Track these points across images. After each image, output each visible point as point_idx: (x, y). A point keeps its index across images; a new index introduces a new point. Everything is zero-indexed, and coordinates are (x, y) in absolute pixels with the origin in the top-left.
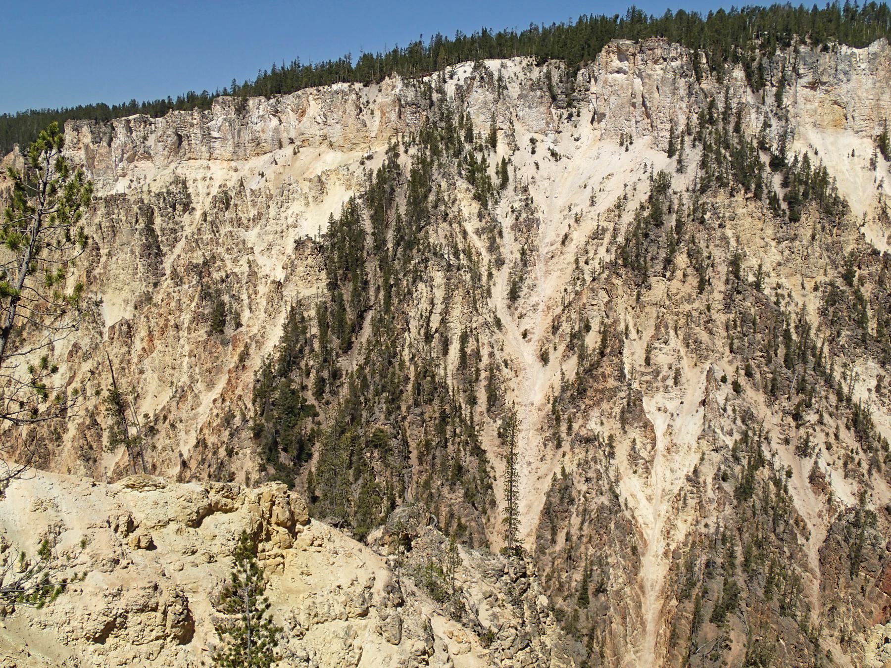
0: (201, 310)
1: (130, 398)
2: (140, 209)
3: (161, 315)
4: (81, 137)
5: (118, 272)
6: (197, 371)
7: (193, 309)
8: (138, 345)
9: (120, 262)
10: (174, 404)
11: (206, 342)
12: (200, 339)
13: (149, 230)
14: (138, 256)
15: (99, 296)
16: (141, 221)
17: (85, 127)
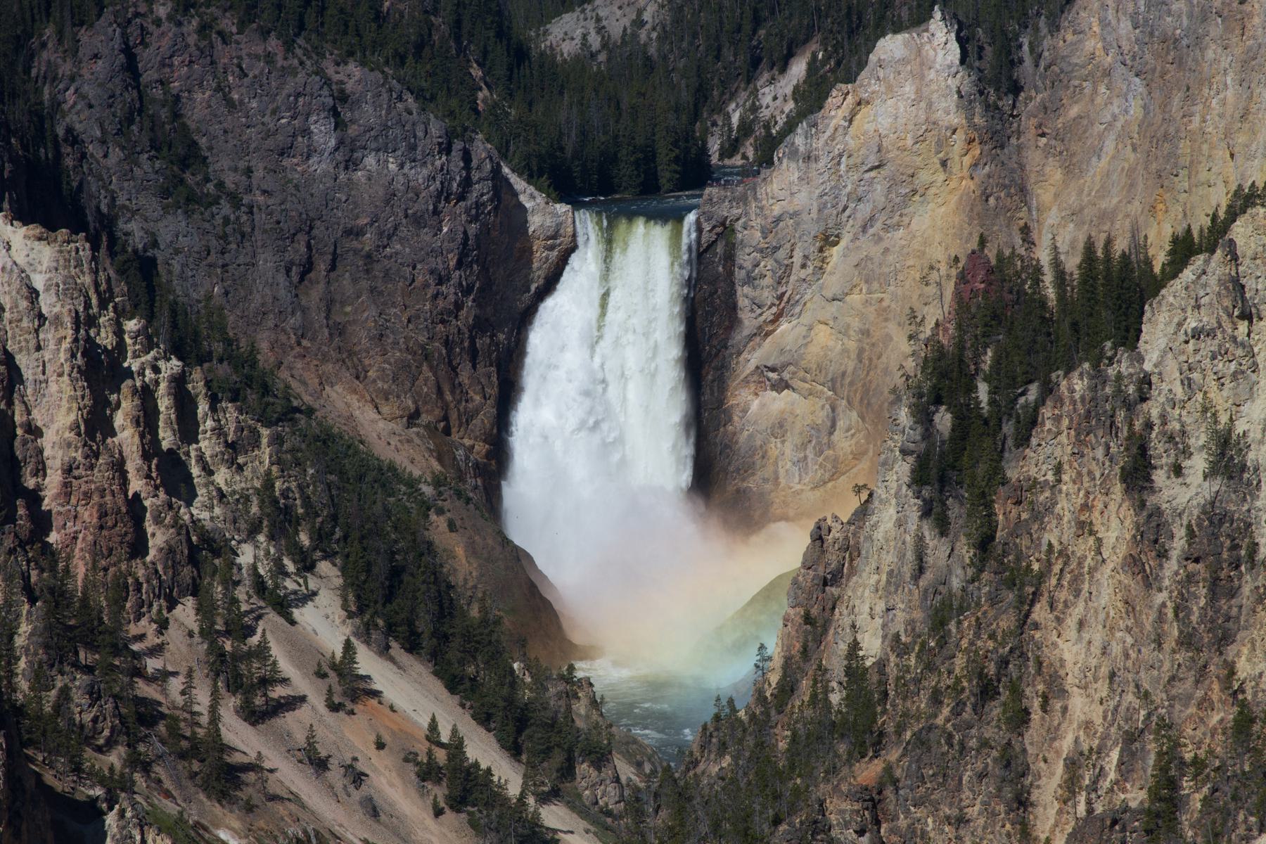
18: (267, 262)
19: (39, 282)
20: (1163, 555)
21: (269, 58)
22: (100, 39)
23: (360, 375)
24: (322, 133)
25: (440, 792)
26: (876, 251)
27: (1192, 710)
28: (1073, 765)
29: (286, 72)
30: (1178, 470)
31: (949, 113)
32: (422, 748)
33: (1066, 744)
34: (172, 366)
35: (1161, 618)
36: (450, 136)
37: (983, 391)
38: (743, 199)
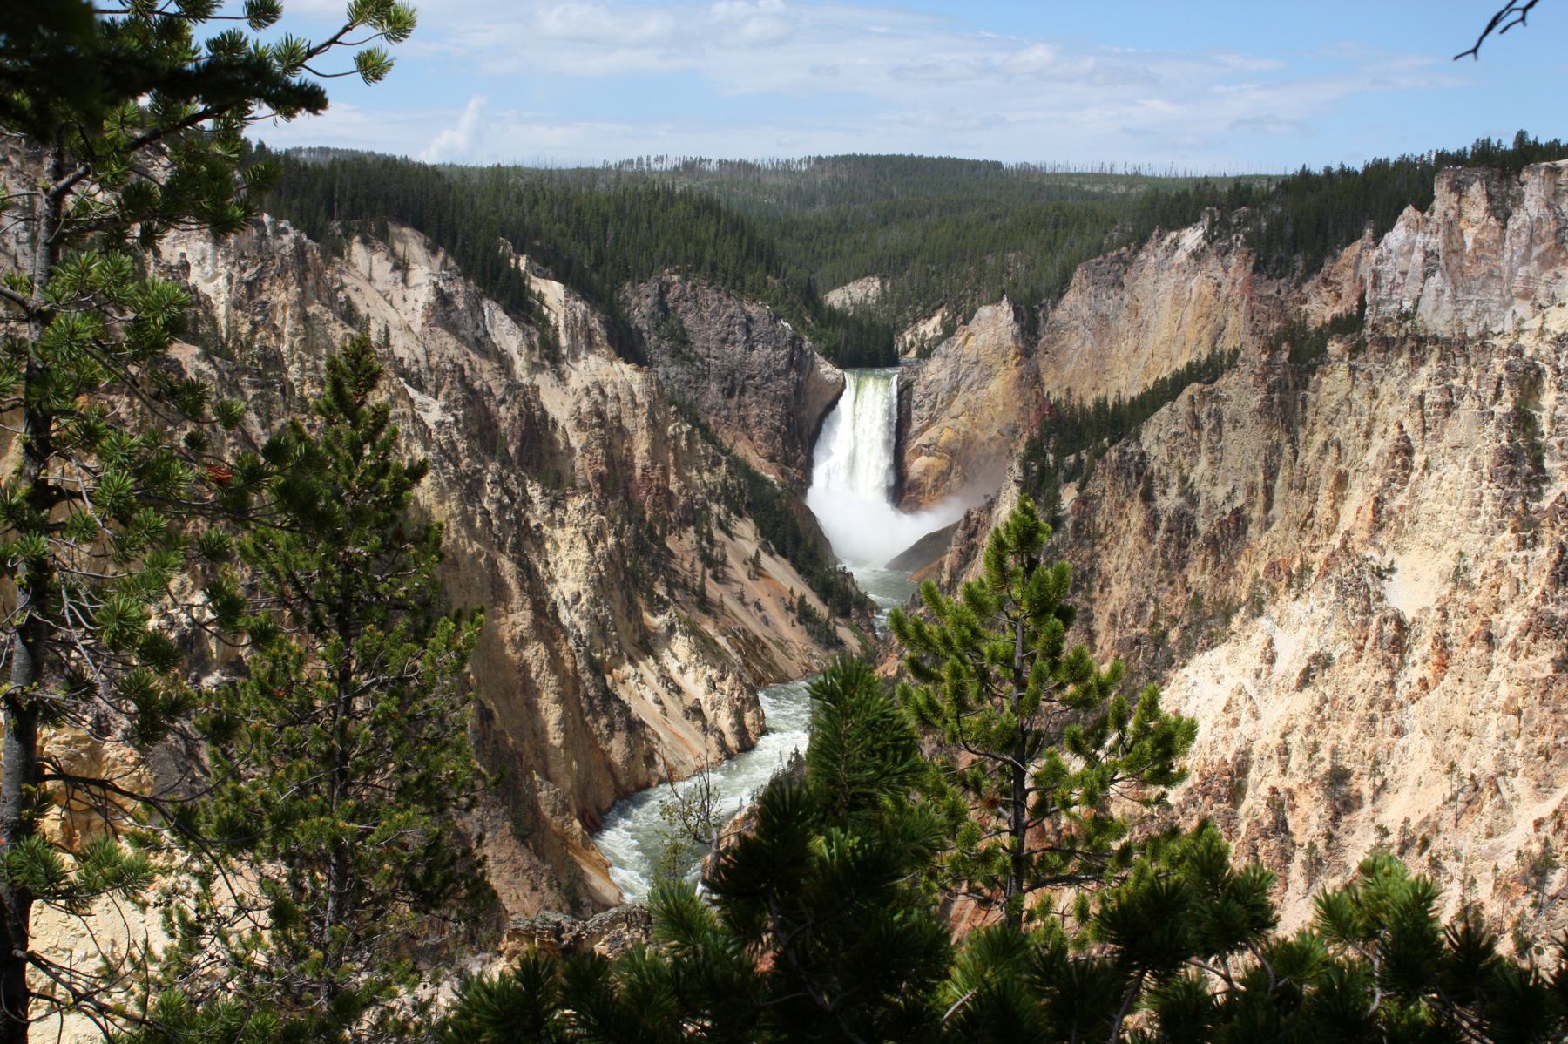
0: (1550, 606)
1: (1365, 787)
2: (1508, 367)
3: (1474, 610)
4: (1465, 206)
5: (1437, 506)
6: (1519, 746)
7: (1532, 603)
8: (1413, 674)
9: (1445, 485)
10: (1449, 814)
11: (1549, 684)
12: (1537, 675)
13: (1523, 419)
14: (1487, 476)
15: (1391, 554)
16: (1506, 395)
17: (1477, 184)
18: (714, 387)
19: (635, 388)
20: (1157, 528)
21: (720, 300)
22: (650, 289)
23: (751, 439)
24: (740, 336)
25: (793, 616)
26: (972, 398)
27: (1167, 594)
28: (1113, 615)
29: (728, 306)
30: (1164, 493)
31: (1008, 342)
32: (788, 597)
33: (1110, 607)
34: (686, 428)
35: (1154, 556)
36: (794, 338)
37: (1050, 457)
38: (917, 373)
